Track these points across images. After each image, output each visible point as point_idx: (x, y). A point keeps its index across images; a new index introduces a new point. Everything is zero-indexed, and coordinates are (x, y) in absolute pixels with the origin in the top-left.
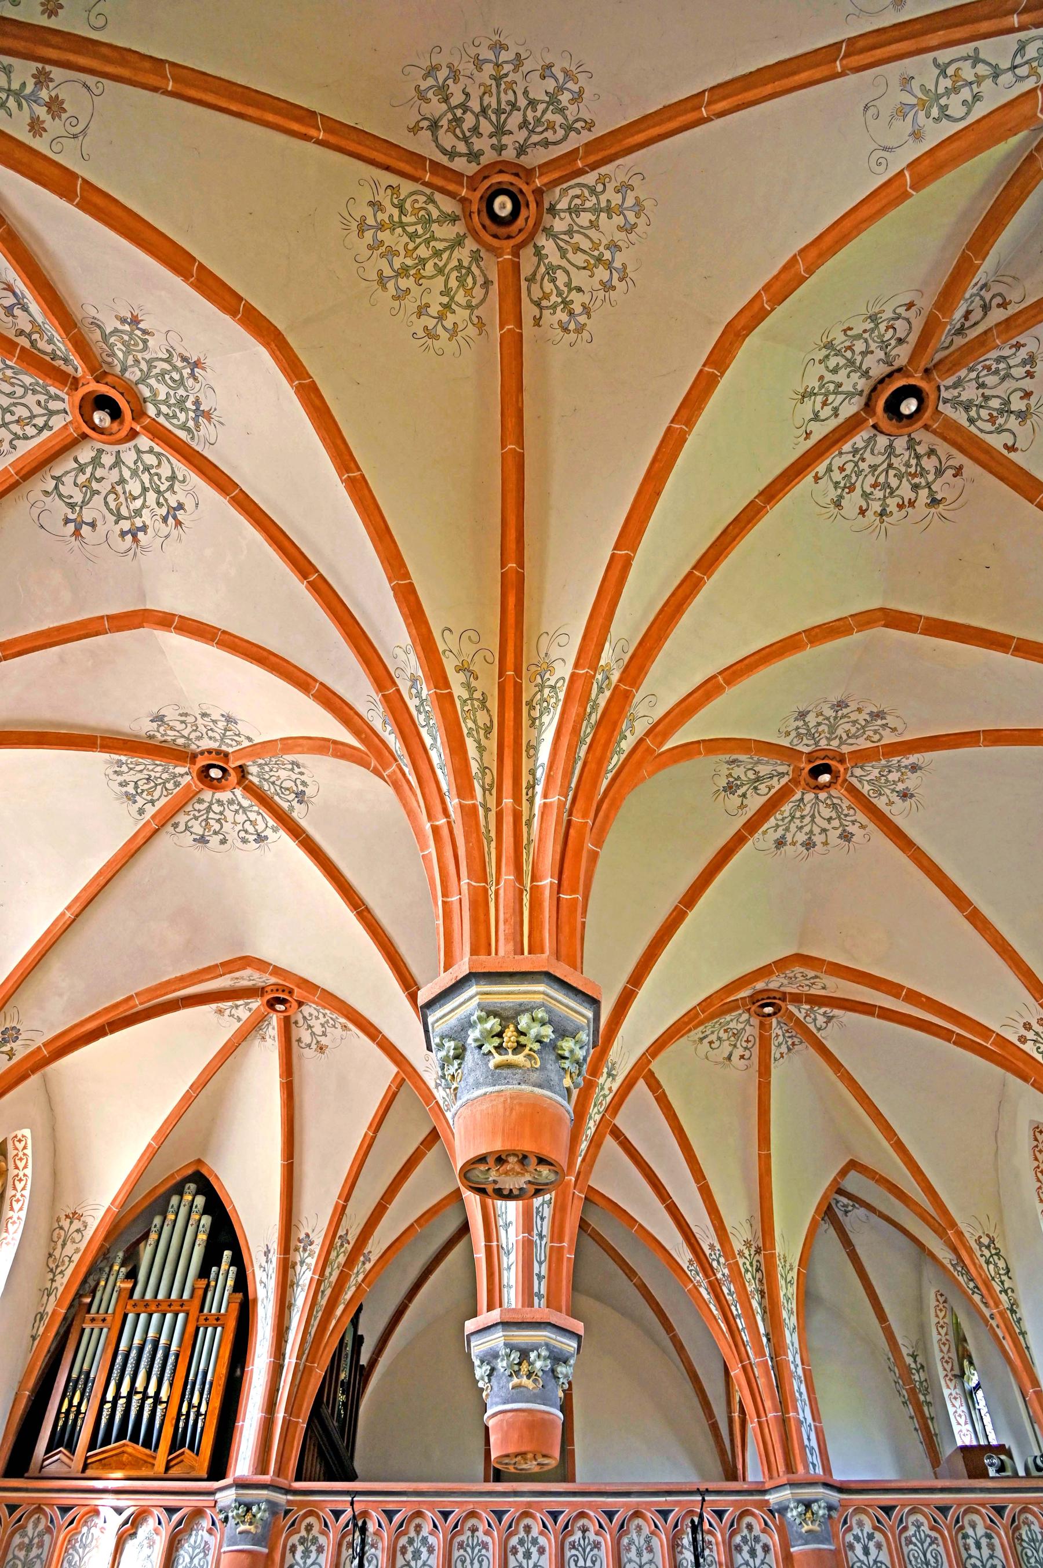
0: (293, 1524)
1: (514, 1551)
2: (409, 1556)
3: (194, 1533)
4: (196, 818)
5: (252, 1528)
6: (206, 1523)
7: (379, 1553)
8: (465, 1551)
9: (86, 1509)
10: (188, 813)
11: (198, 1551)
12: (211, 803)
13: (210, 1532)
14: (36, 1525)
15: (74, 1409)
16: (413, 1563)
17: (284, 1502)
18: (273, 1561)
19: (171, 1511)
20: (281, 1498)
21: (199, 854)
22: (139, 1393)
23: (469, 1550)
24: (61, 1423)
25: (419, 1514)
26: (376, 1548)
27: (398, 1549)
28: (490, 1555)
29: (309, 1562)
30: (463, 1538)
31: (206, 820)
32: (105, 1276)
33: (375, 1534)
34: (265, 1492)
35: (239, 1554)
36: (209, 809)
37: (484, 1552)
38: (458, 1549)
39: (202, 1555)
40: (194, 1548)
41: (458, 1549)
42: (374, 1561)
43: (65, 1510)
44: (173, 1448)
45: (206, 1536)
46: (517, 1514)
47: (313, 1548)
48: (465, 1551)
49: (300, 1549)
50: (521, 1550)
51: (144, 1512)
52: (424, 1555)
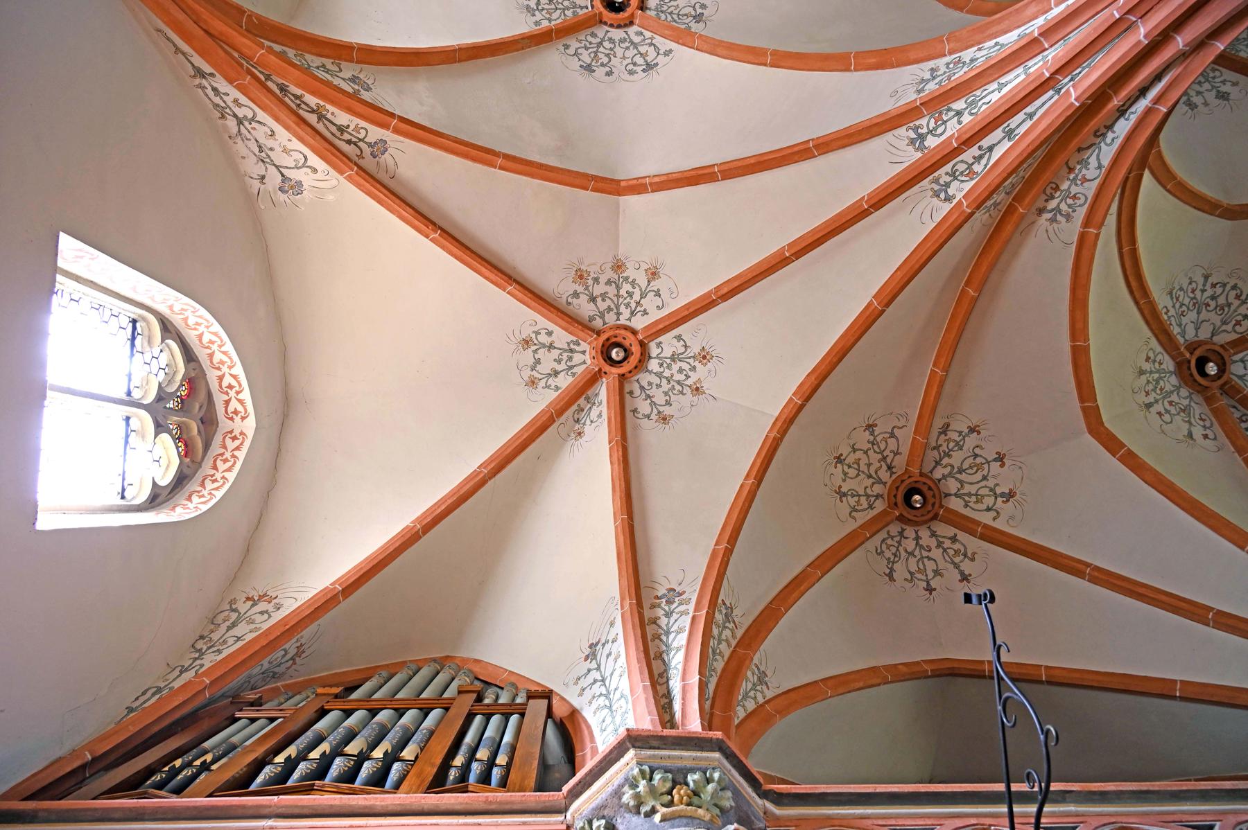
4: (587, 49)
10: (580, 41)
12: (603, 40)
21: (582, 80)
31: (596, 53)
36: (600, 44)
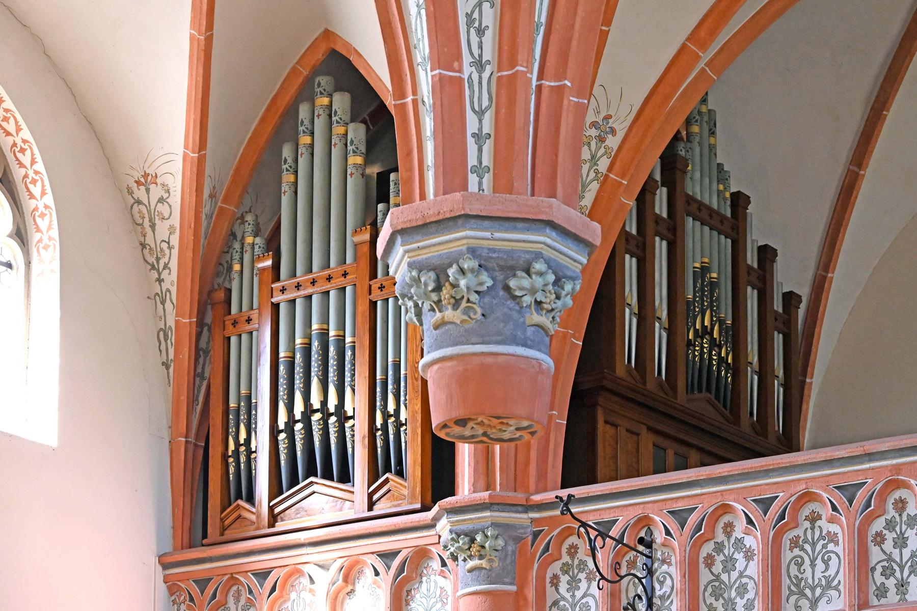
0: (547, 549)
1: (880, 539)
2: (718, 568)
3: (424, 579)
5: (484, 563)
6: (436, 565)
7: (672, 570)
8: (802, 549)
9: (287, 569)
11: (433, 600)
13: (442, 574)
14: (237, 600)
15: (242, 449)
16: (724, 577)
17: (528, 523)
18: (525, 599)
19: (387, 556)
20: (523, 518)
22: (317, 411)
23: (808, 547)
24: (232, 470)
25: (725, 509)
26: (669, 564)
27: (701, 560)
28: (839, 550)
29: (579, 594)
30: (799, 532)
32: (237, 256)
33: (663, 545)
34: (487, 514)
35: (474, 597)
37: (831, 547)
38: (791, 549)
39: (439, 605)
40: (427, 597)
41: (791, 549)
42: (668, 582)
43: (262, 575)
44: (373, 476)
45: (441, 581)
46: (879, 487)
47: (582, 576)
48: (802, 549)
49: (564, 579)
50: (890, 536)
51: (357, 562)
52: (741, 563)
